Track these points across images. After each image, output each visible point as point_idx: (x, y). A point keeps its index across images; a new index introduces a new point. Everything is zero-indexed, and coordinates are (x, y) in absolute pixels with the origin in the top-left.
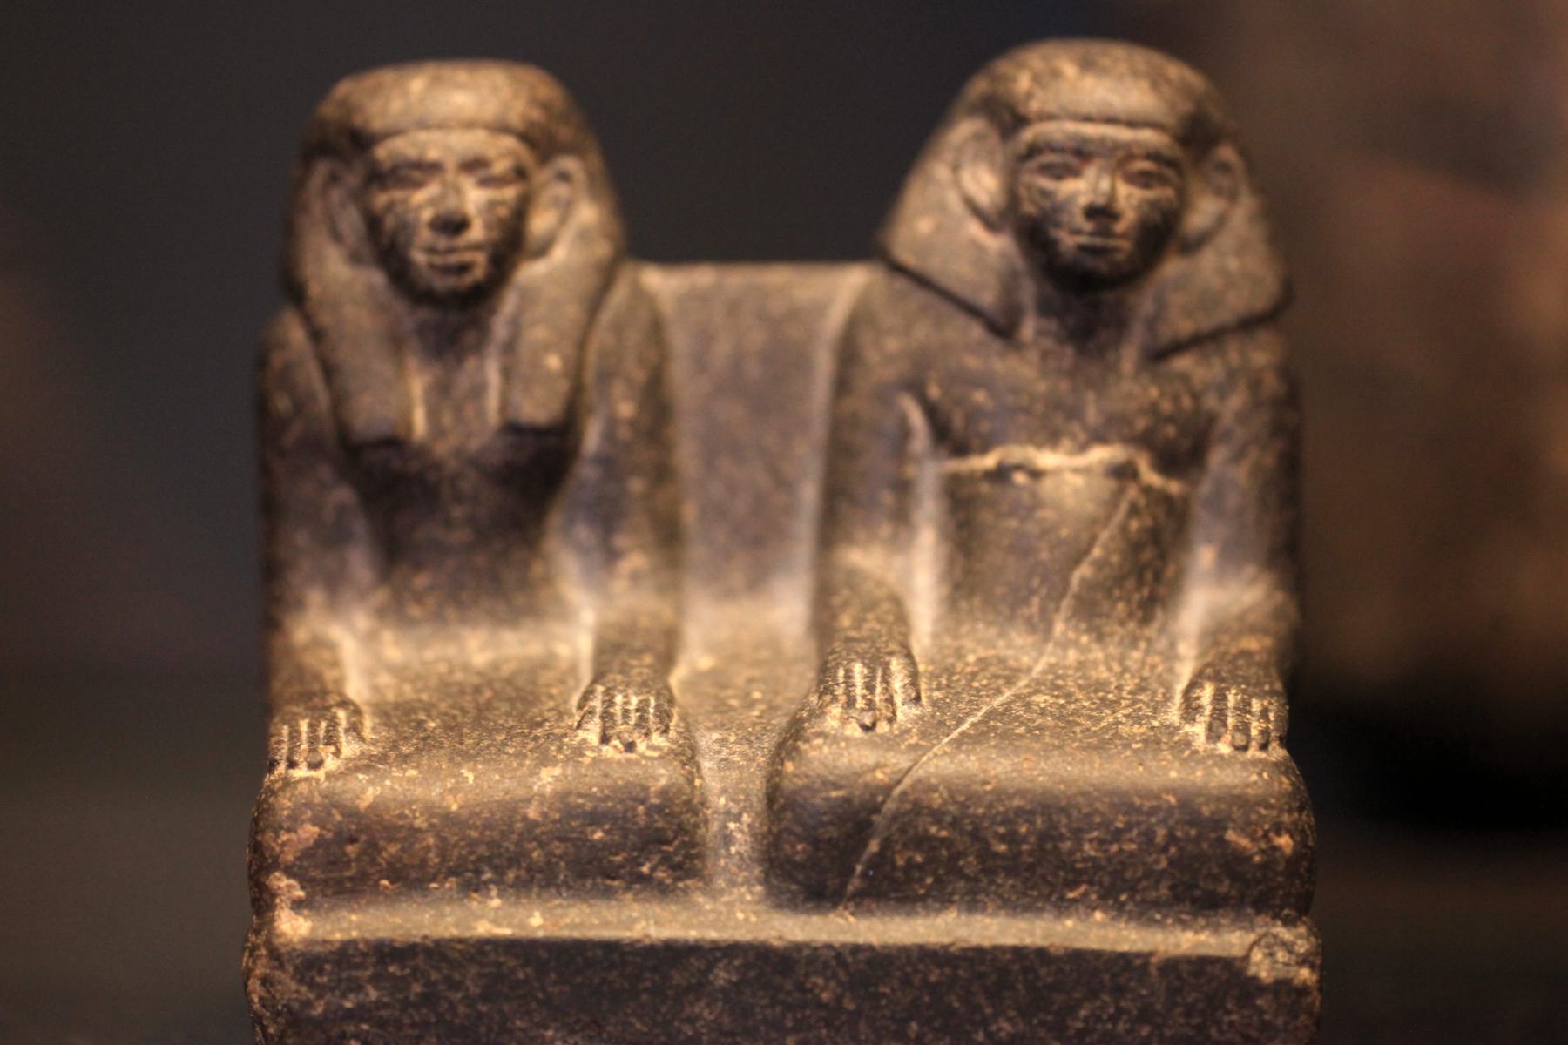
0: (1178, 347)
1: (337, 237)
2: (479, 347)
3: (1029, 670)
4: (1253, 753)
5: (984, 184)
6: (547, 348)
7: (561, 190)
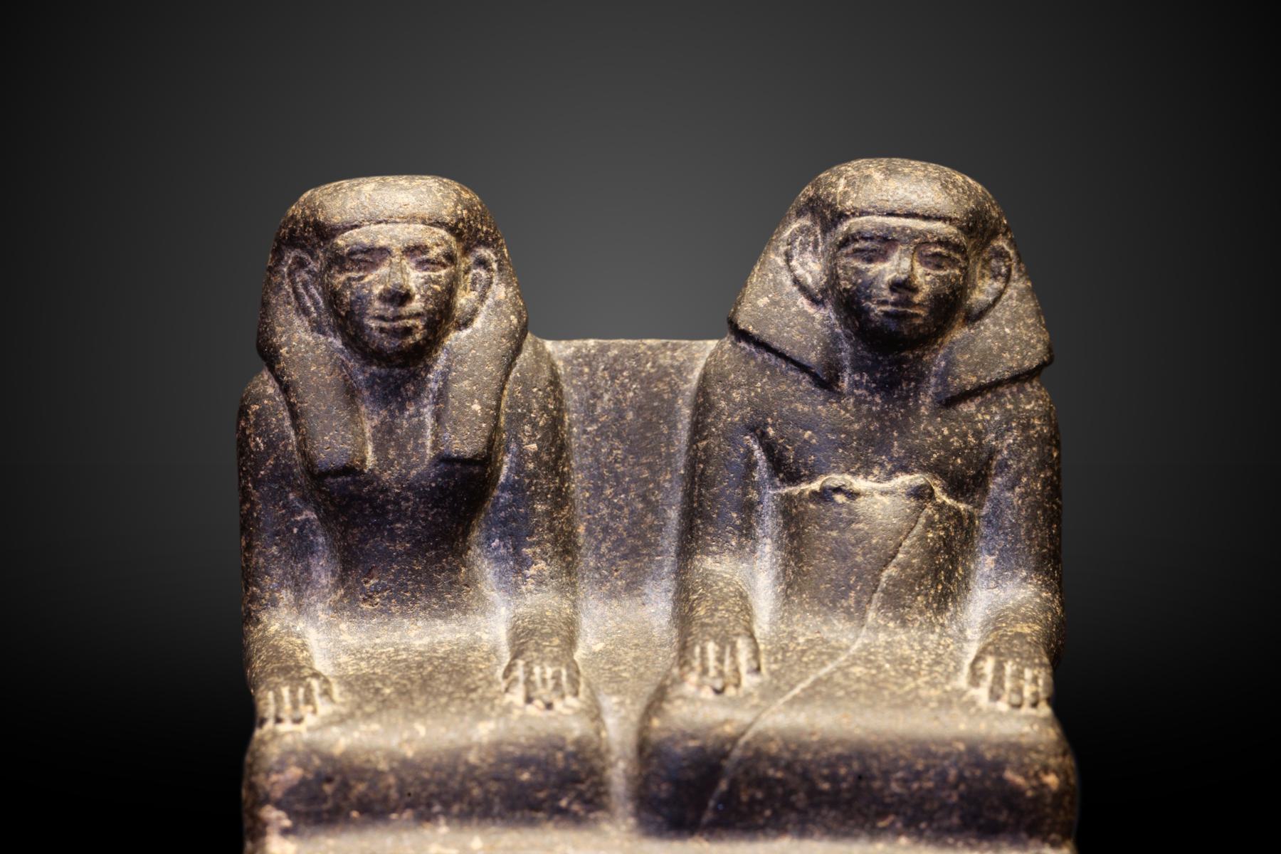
0: (966, 396)
1: (305, 311)
2: (417, 395)
3: (848, 648)
4: (1026, 710)
5: (811, 268)
6: (472, 396)
7: (483, 273)
